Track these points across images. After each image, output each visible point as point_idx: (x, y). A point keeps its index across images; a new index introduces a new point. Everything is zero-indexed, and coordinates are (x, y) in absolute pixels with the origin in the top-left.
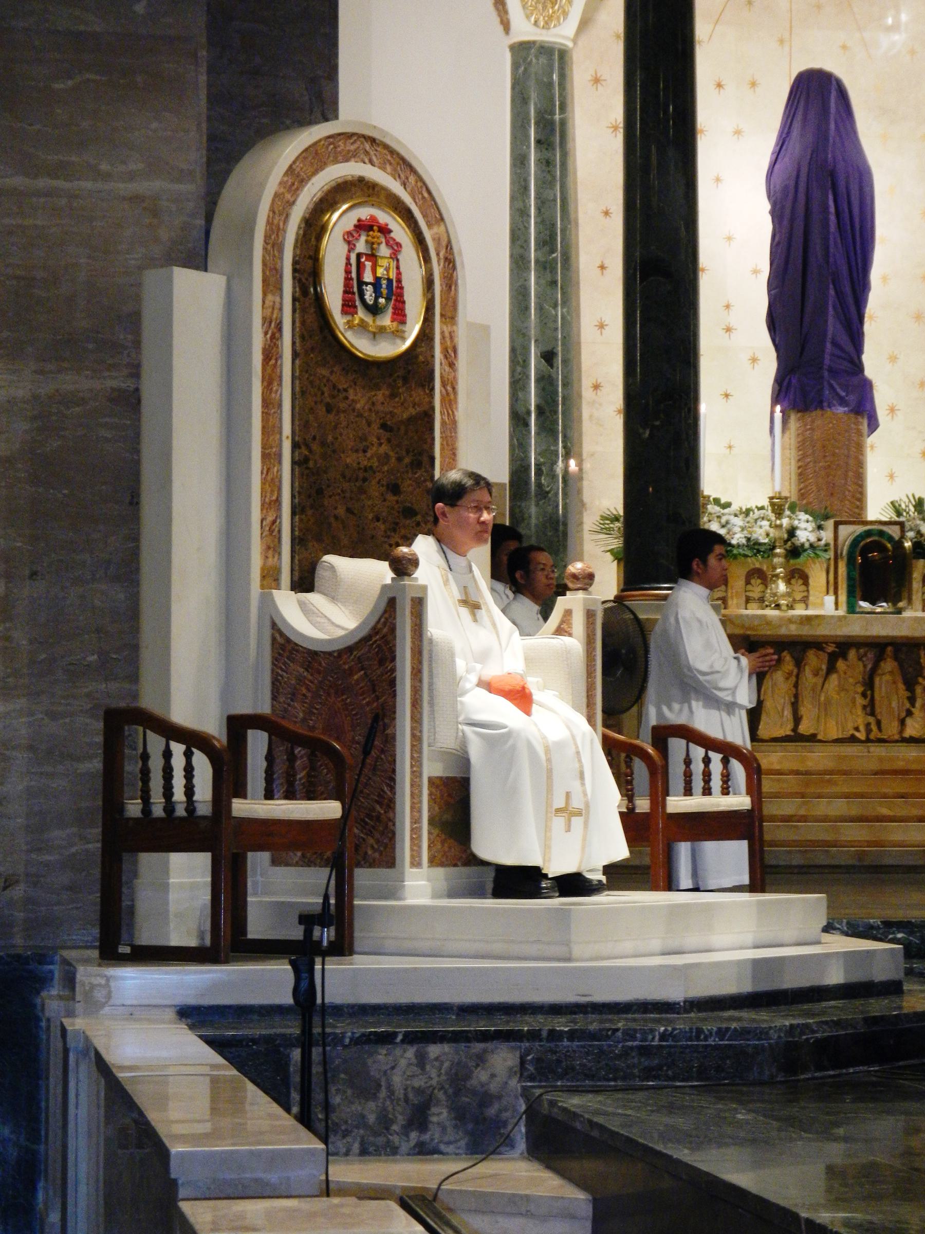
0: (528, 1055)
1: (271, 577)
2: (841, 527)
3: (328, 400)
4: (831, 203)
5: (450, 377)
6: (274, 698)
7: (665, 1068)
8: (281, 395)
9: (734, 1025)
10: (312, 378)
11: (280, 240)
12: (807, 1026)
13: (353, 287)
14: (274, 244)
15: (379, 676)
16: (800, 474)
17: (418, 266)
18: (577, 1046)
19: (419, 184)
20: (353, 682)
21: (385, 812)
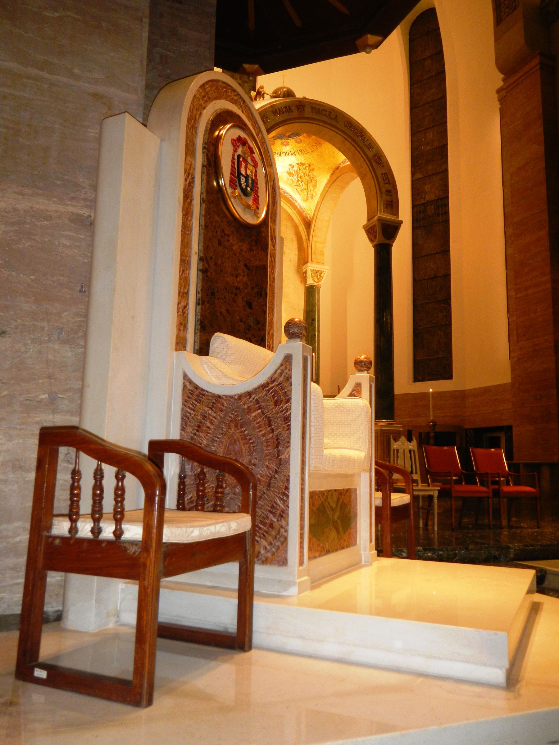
1: (180, 345)
3: (219, 237)
6: (183, 429)
10: (211, 219)
15: (275, 413)
20: (251, 418)
21: (278, 521)
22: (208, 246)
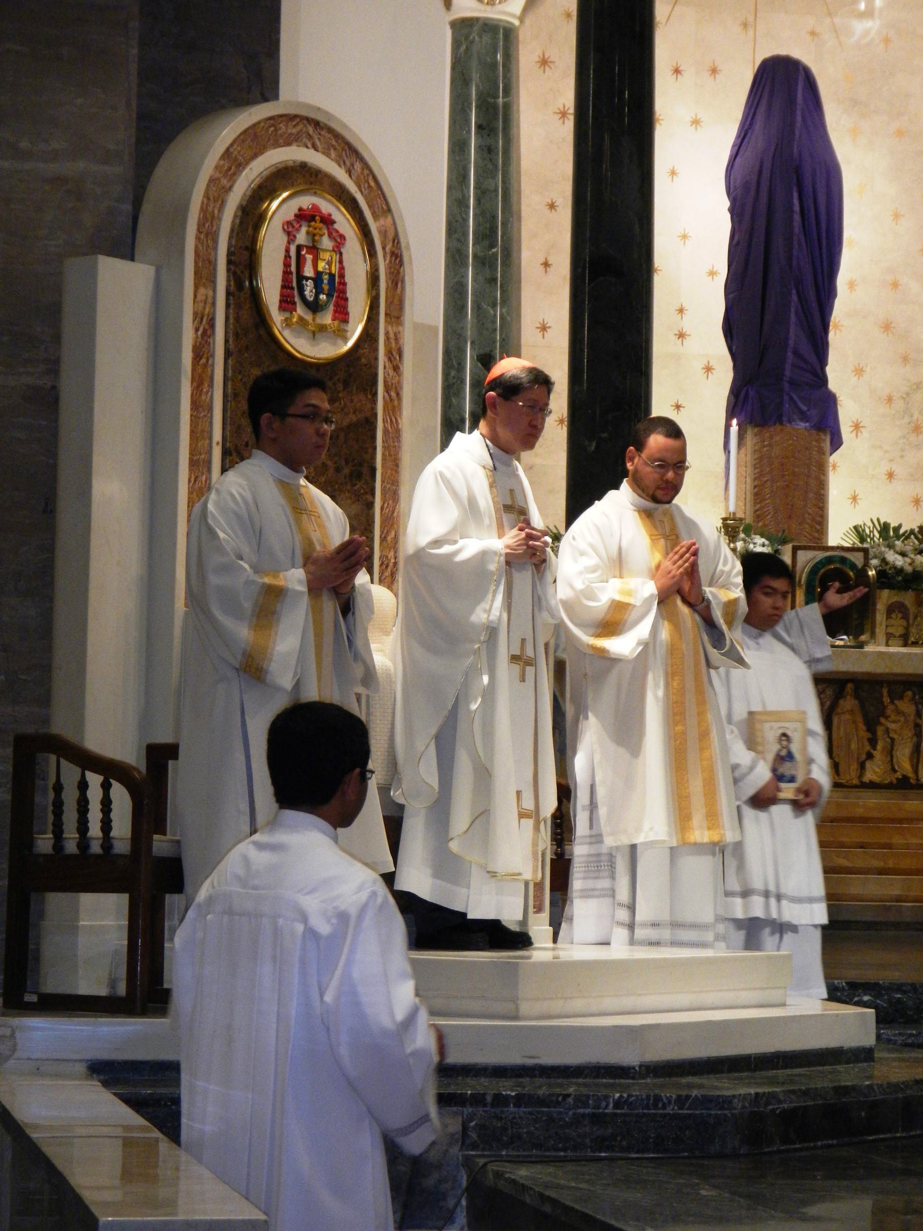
0: (472, 1122)
2: (800, 553)
4: (796, 202)
5: (393, 382)
7: (619, 1138)
8: (212, 397)
9: (695, 1093)
11: (214, 228)
12: (772, 1096)
13: (291, 282)
14: (207, 233)
16: (756, 494)
17: (363, 261)
18: (524, 1112)
19: (366, 172)
22: (239, 427)
